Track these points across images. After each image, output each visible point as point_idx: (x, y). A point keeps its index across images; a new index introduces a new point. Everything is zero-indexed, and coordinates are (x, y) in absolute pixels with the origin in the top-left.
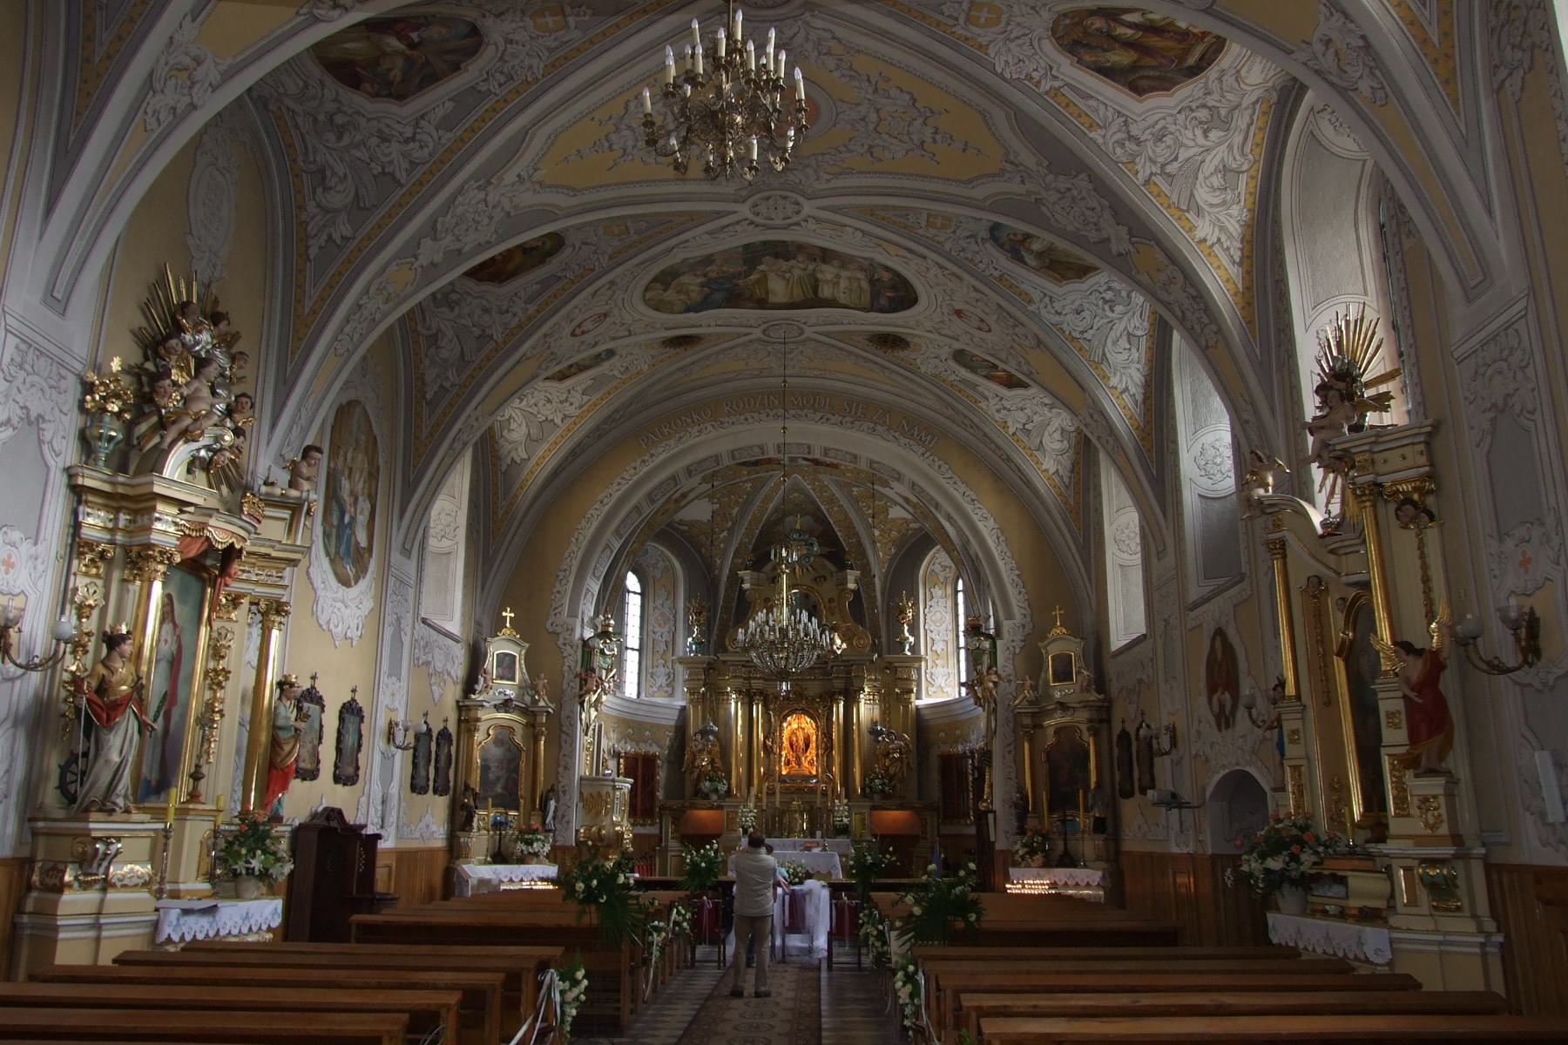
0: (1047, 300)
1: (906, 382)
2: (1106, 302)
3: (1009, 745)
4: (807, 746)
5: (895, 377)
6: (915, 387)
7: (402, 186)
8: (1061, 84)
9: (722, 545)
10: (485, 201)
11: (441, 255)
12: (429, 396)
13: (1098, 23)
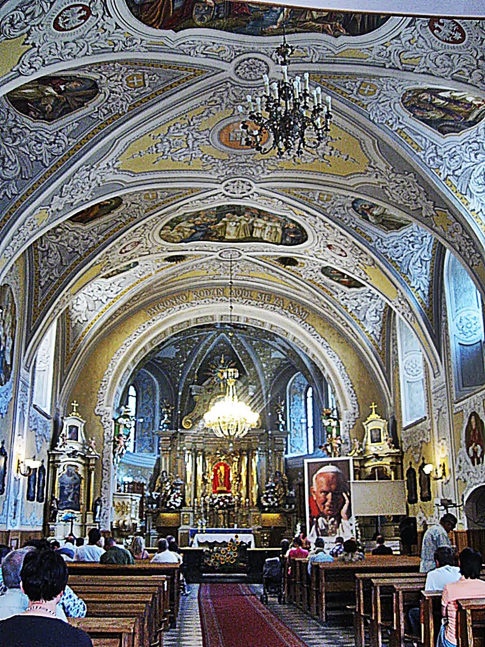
0: (379, 240)
1: (294, 284)
2: (410, 242)
5: (287, 280)
6: (298, 286)
7: (46, 167)
8: (403, 127)
10: (89, 177)
11: (63, 206)
12: (42, 284)
13: (427, 96)
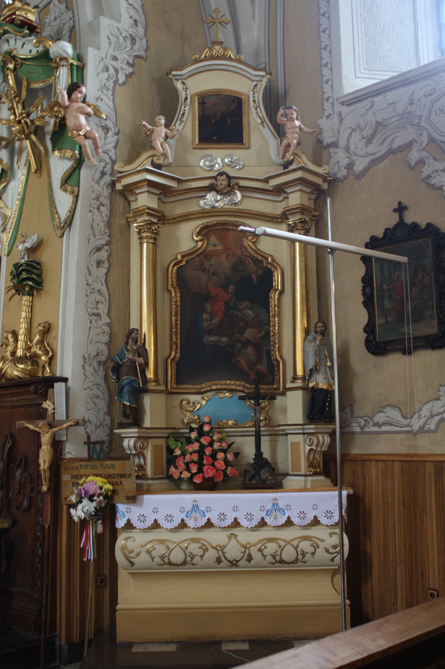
3: (99, 249)
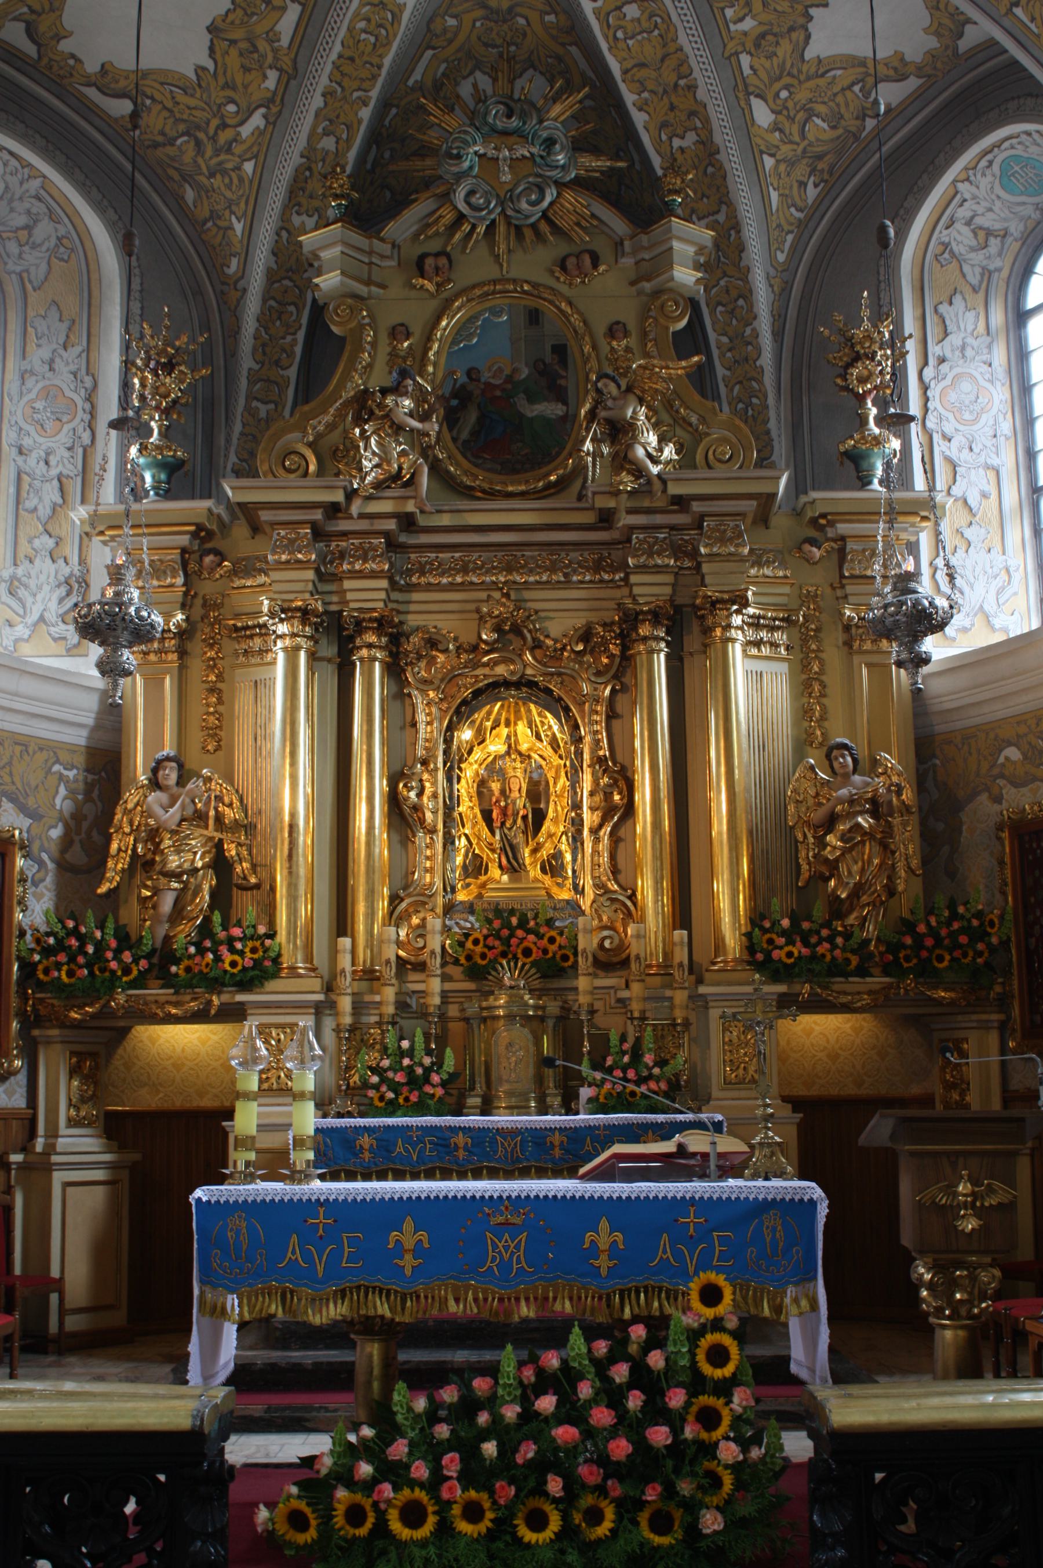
4: (539, 817)
9: (249, 167)
